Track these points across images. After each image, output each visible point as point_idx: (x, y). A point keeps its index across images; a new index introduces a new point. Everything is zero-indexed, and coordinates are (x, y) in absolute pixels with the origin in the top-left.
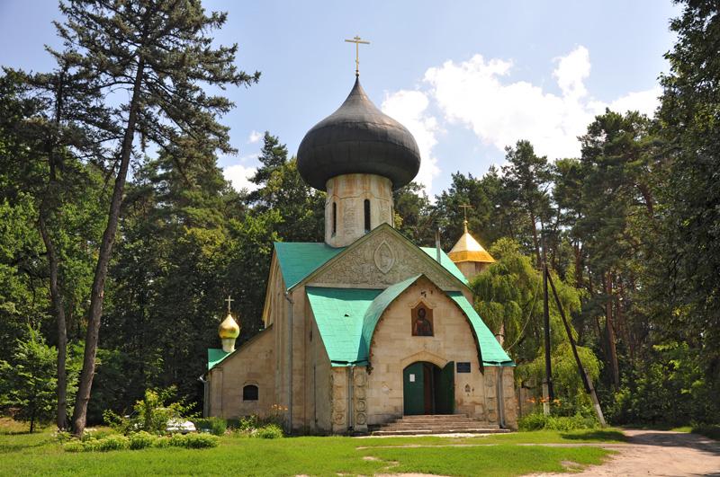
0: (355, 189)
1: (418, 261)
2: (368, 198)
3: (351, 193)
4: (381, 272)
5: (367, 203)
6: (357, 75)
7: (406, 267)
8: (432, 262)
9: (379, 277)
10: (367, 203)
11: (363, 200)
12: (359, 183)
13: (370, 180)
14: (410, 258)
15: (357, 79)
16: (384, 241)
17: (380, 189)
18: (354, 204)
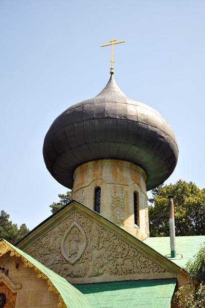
0: (86, 179)
1: (116, 242)
2: (98, 185)
3: (82, 183)
4: (68, 262)
5: (98, 190)
6: (112, 73)
7: (102, 252)
8: (132, 240)
9: (65, 269)
10: (98, 190)
11: (93, 189)
12: (90, 172)
13: (102, 167)
14: (107, 240)
15: (111, 76)
16: (75, 223)
17: (115, 174)
18: (84, 194)
